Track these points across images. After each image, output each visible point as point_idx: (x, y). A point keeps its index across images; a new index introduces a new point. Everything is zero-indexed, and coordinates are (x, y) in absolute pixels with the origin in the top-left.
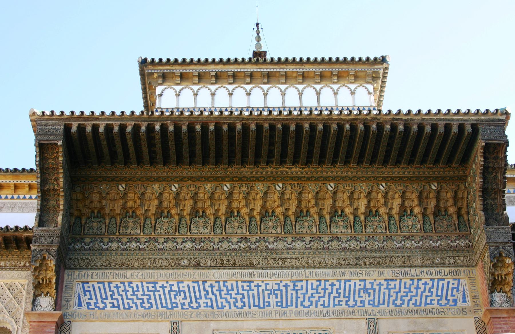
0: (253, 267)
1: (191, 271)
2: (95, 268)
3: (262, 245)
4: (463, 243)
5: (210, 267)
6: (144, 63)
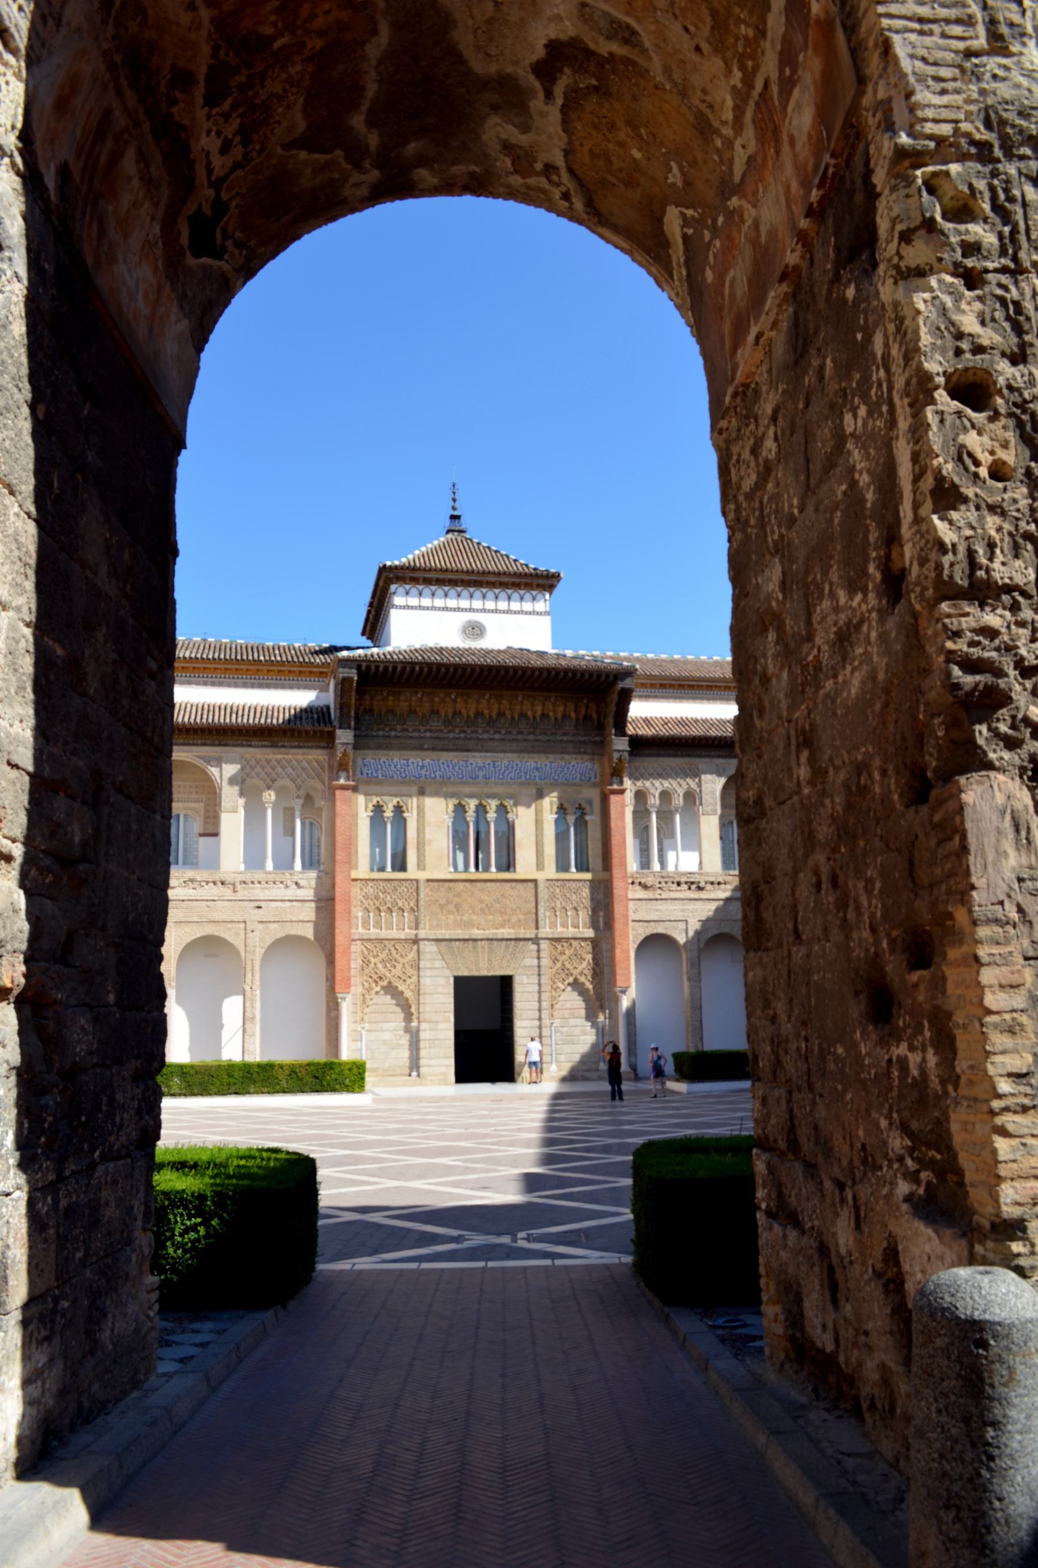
0: (468, 750)
1: (429, 753)
2: (369, 748)
3: (474, 735)
4: (598, 739)
5: (442, 750)
6: (383, 570)
